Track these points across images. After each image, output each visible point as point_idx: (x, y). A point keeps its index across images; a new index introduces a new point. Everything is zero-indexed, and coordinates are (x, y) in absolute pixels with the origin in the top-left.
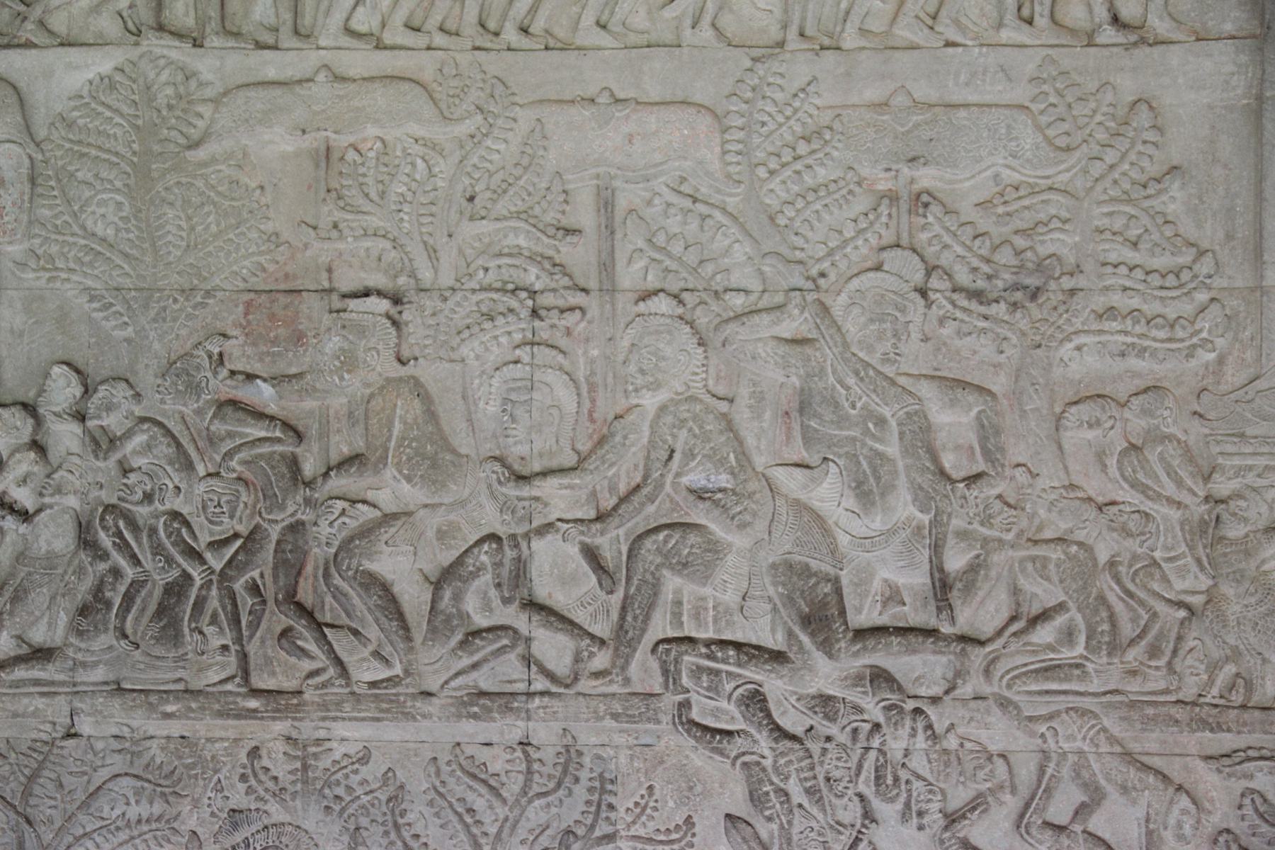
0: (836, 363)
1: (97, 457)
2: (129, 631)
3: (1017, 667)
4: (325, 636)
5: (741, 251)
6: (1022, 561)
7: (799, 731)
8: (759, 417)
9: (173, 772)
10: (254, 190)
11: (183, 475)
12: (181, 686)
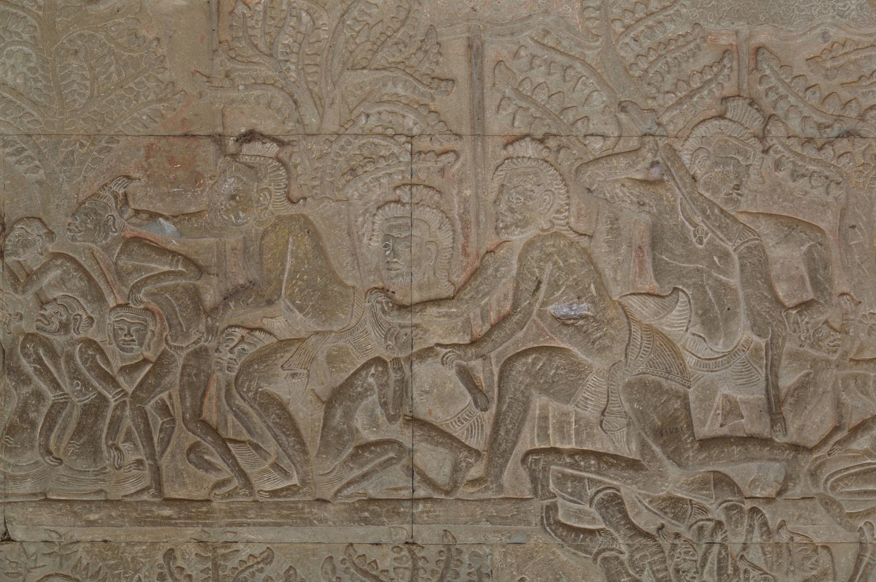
0: (685, 202)
1: (16, 290)
2: (52, 448)
3: (840, 471)
4: (230, 451)
5: (599, 99)
6: (844, 379)
7: (652, 529)
8: (616, 251)
9: (98, 572)
10: (151, 42)
11: (95, 306)
12: (101, 497)
